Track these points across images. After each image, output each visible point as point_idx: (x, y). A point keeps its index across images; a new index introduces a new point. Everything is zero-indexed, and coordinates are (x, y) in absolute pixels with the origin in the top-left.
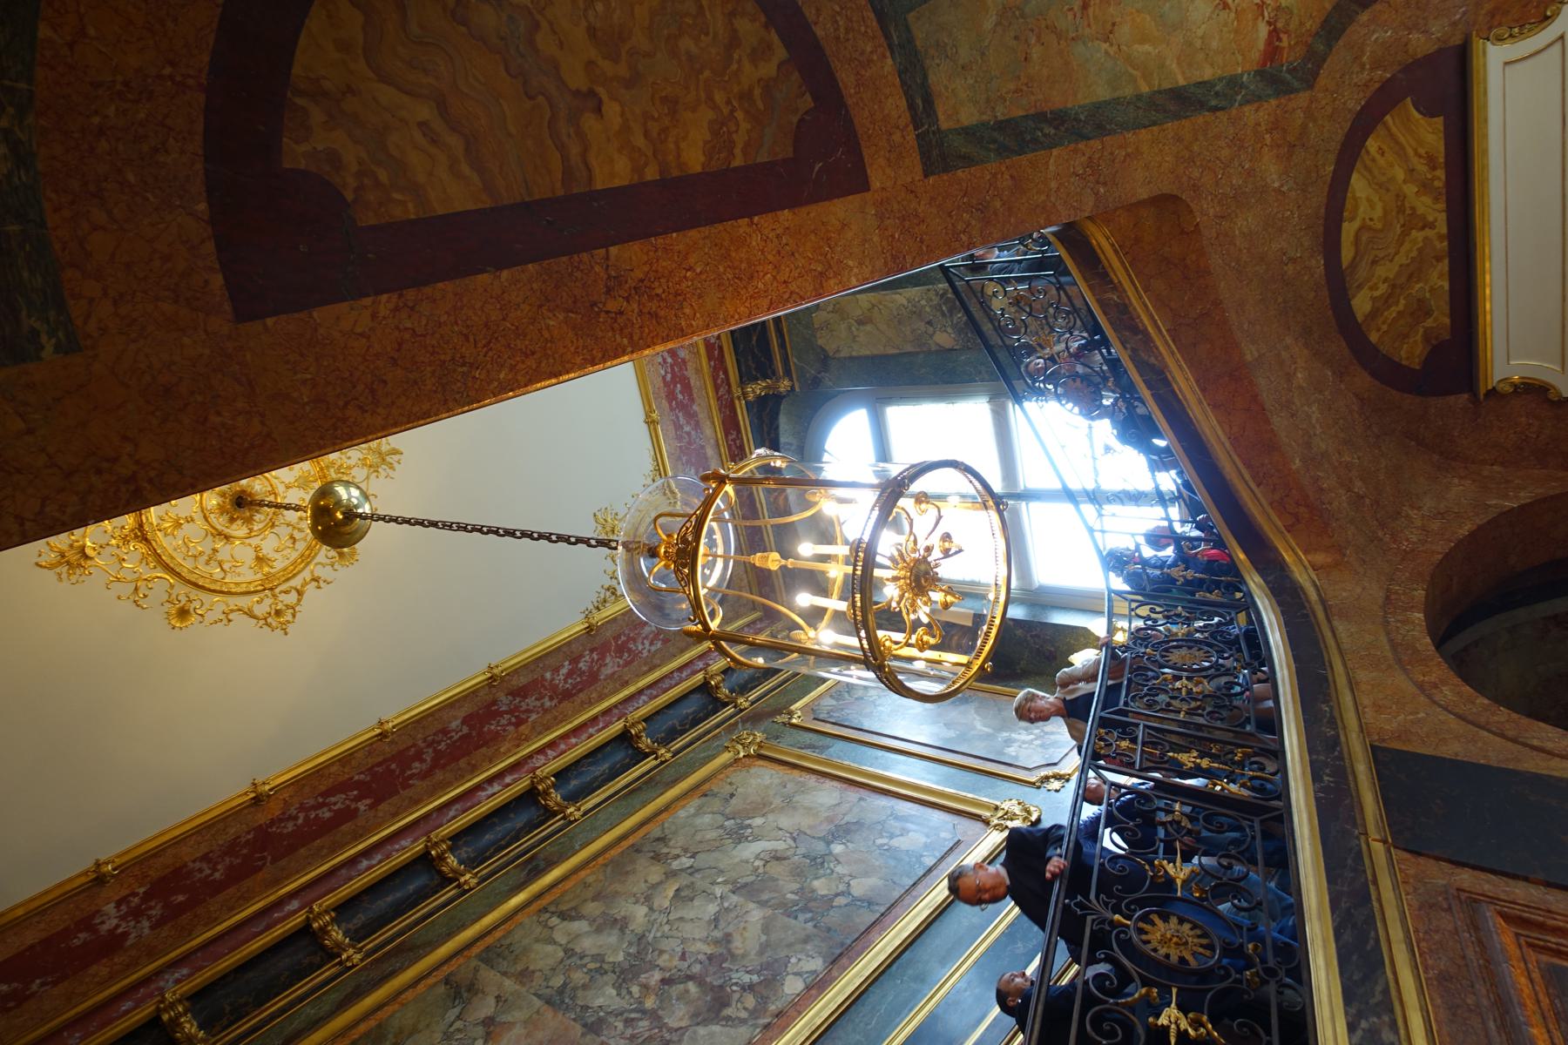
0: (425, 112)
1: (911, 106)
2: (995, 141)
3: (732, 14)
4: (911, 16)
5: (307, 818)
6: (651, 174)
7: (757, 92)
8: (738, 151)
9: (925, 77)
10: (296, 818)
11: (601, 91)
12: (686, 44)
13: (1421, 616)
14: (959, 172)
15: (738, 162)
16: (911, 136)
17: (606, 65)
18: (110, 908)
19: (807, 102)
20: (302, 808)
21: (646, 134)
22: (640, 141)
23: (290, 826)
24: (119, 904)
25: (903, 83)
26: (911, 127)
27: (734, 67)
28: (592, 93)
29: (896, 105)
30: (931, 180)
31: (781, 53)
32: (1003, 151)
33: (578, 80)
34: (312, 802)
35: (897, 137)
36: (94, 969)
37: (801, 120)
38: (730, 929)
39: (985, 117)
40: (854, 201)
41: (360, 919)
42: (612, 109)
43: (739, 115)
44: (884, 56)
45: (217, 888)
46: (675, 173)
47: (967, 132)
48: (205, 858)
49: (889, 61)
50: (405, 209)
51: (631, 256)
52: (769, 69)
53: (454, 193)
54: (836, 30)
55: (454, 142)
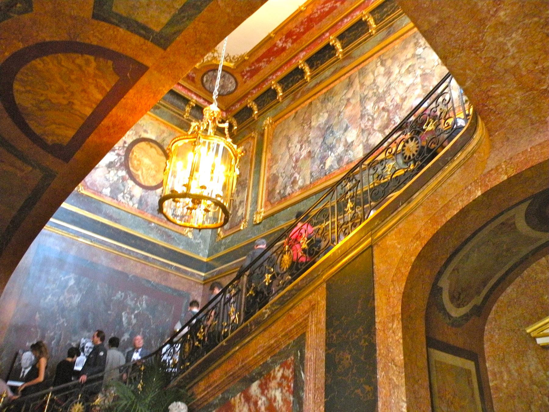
0: (54, 126)
1: (141, 35)
2: (184, 17)
3: (73, 62)
4: (114, 9)
5: (321, 12)
6: (94, 106)
7: (97, 72)
8: (106, 87)
9: (137, 22)
10: (317, 12)
11: (70, 100)
12: (73, 77)
13: (479, 193)
14: (178, 38)
15: (108, 90)
16: (149, 43)
17: (65, 96)
18: (278, 42)
19: (110, 63)
20: (317, 9)
21: (85, 100)
22: (86, 102)
23: (317, 15)
24: (280, 40)
25: (132, 31)
26: (146, 41)
27: (86, 72)
28: (70, 102)
29: (136, 39)
30: (168, 49)
31: (92, 58)
32: (190, 18)
33: (65, 102)
34: (320, 7)
35: (145, 48)
36: (282, 54)
37: (113, 68)
38: (408, 95)
39: (172, 13)
40: (147, 73)
41: (346, 40)
42: (75, 101)
43: (98, 80)
44: (118, 30)
45: (304, 33)
46: (99, 102)
47: (169, 24)
48: (296, 27)
49: (121, 30)
50: (68, 140)
51: (106, 122)
52: (94, 64)
53: (71, 133)
54: (98, 38)
55: (62, 126)
